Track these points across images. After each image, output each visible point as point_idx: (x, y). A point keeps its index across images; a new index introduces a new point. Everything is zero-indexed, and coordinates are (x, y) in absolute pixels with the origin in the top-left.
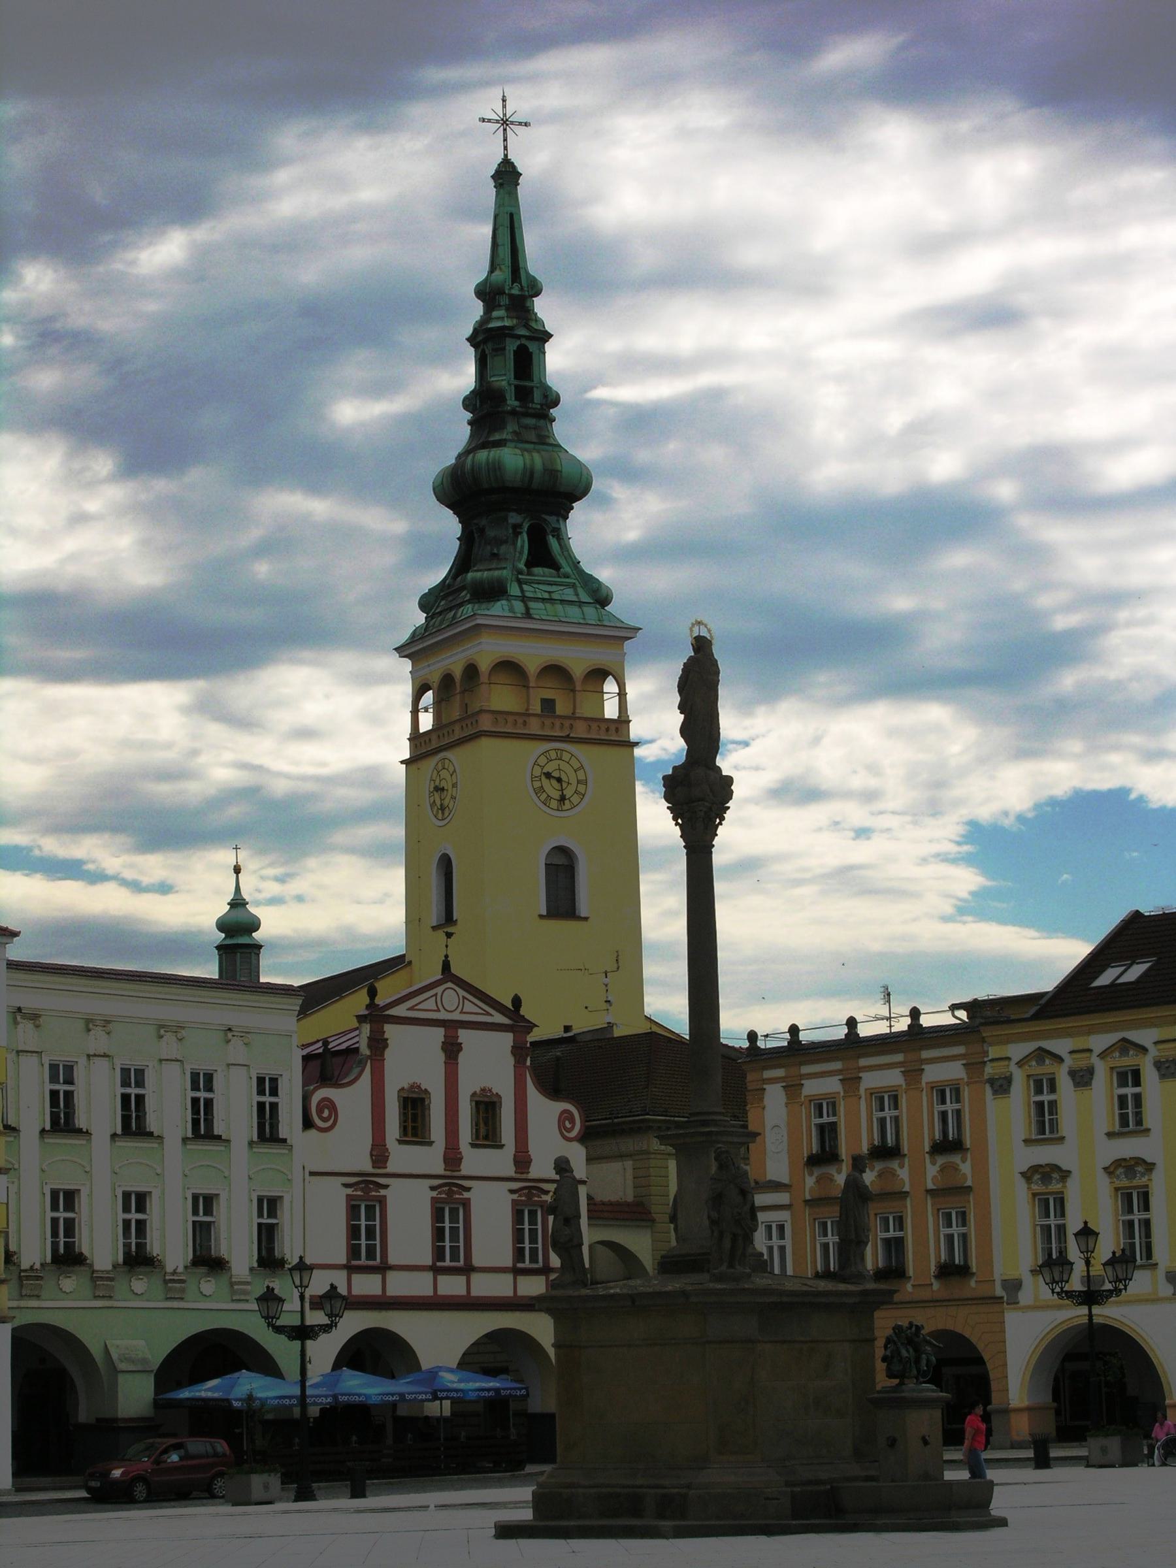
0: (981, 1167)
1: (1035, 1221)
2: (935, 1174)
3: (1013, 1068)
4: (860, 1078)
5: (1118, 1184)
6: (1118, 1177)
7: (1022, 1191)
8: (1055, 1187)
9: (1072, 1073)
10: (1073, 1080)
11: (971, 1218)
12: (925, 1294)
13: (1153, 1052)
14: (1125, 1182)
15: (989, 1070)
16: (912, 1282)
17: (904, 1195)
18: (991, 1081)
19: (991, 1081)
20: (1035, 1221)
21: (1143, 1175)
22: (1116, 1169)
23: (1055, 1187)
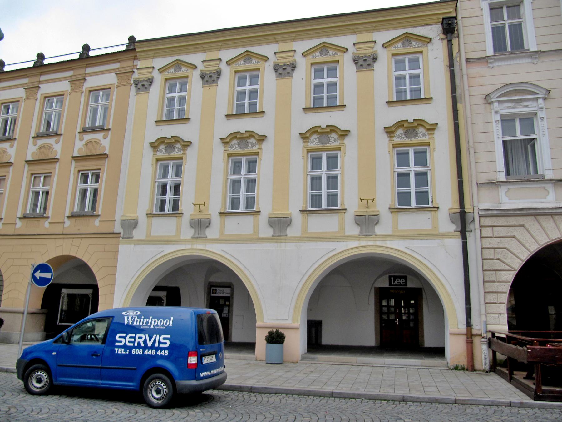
0: (118, 144)
1: (155, 179)
2: (81, 146)
3: (156, 74)
4: (40, 87)
5: (231, 151)
6: (232, 147)
7: (148, 156)
8: (177, 153)
9: (203, 76)
10: (203, 79)
11: (103, 178)
12: (58, 229)
13: (273, 59)
14: (237, 150)
15: (136, 76)
16: (49, 220)
17: (55, 160)
18: (136, 83)
19: (136, 83)
20: (155, 179)
21: (254, 145)
22: (231, 140)
23: (177, 153)
